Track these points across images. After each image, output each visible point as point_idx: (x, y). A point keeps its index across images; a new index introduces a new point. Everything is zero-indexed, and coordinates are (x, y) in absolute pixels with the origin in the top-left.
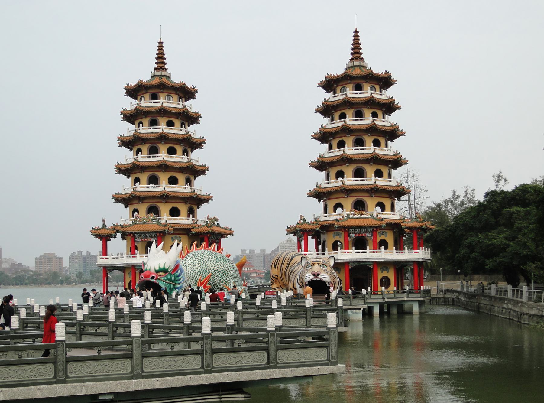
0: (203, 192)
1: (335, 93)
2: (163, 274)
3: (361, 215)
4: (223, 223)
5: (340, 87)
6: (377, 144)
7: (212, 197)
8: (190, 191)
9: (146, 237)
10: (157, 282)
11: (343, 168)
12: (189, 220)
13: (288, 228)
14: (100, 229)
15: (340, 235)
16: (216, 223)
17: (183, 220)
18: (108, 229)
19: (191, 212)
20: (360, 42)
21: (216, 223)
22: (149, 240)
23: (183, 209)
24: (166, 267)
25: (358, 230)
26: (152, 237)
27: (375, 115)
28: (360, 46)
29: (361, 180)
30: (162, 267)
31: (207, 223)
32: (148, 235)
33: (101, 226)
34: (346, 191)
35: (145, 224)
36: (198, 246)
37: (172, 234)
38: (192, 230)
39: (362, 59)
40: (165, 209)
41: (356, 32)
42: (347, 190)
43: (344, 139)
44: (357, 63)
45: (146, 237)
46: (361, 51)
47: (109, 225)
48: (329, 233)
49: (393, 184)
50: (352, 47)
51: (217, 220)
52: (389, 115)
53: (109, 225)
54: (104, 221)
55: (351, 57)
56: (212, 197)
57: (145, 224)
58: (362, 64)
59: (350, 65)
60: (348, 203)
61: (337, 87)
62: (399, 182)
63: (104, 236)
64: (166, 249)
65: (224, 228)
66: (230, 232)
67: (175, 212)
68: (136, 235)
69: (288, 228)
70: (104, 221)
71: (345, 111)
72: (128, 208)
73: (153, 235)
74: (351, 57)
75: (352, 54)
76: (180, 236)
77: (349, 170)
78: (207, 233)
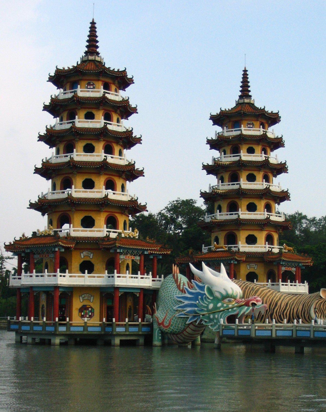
1: (65, 90)
6: (109, 150)
20: (97, 34)
27: (108, 117)
28: (97, 39)
39: (98, 54)
41: (93, 23)
44: (90, 58)
46: (97, 44)
49: (125, 198)
50: (88, 38)
52: (126, 118)
55: (86, 49)
58: (98, 59)
59: (86, 59)
62: (133, 196)
74: (86, 49)
75: (87, 47)
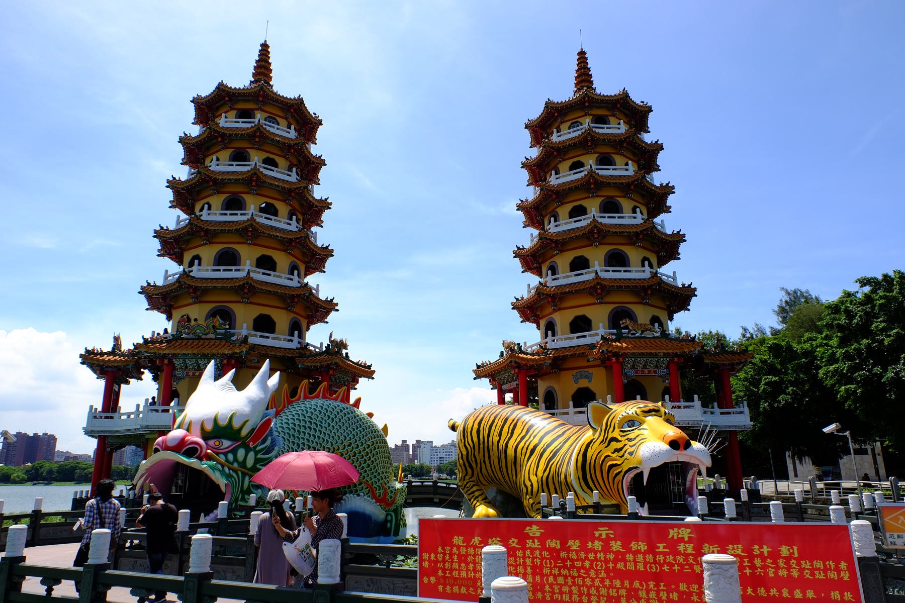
2: (226, 443)
3: (643, 332)
5: (569, 123)
7: (336, 305)
10: (204, 466)
11: (586, 252)
12: (292, 341)
13: (478, 367)
14: (102, 354)
15: (588, 377)
16: (344, 352)
18: (123, 355)
19: (297, 329)
21: (344, 352)
24: (236, 425)
25: (642, 361)
29: (625, 271)
30: (223, 423)
33: (107, 347)
34: (599, 290)
36: (312, 390)
38: (297, 360)
42: (603, 287)
43: (584, 203)
48: (563, 373)
54: (117, 339)
56: (336, 305)
60: (599, 315)
61: (562, 123)
63: (113, 368)
64: (240, 383)
65: (357, 364)
66: (367, 372)
67: (264, 324)
69: (478, 367)
70: (117, 339)
71: (582, 159)
77: (596, 256)
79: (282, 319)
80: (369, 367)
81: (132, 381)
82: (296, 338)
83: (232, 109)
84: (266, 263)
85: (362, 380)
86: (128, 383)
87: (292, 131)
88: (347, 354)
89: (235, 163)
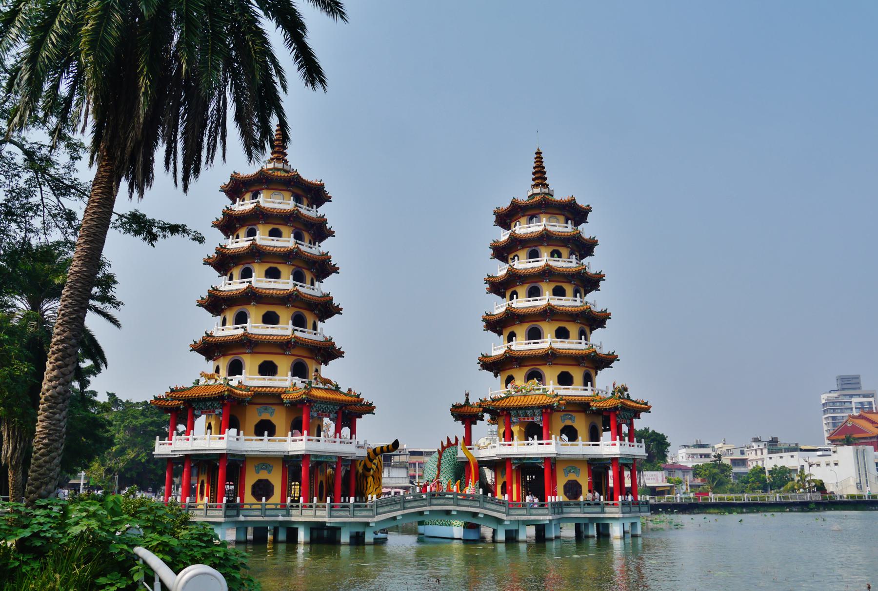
0: (604, 351)
4: (636, 394)
8: (587, 347)
9: (527, 415)
14: (461, 406)
16: (626, 393)
17: (576, 391)
19: (588, 379)
22: (530, 420)
23: (577, 374)
26: (534, 415)
31: (613, 394)
32: (529, 412)
35: (525, 396)
37: (563, 411)
40: (551, 374)
45: (527, 415)
47: (474, 400)
51: (626, 389)
53: (474, 400)
54: (467, 395)
57: (525, 396)
65: (636, 402)
67: (565, 379)
68: (513, 413)
70: (467, 395)
72: (499, 377)
73: (537, 412)
76: (574, 414)
78: (616, 408)
79: (577, 374)
80: (646, 404)
81: (478, 422)
82: (589, 387)
83: (523, 216)
84: (562, 334)
85: (642, 415)
86: (475, 424)
87: (569, 225)
88: (628, 395)
89: (531, 260)
